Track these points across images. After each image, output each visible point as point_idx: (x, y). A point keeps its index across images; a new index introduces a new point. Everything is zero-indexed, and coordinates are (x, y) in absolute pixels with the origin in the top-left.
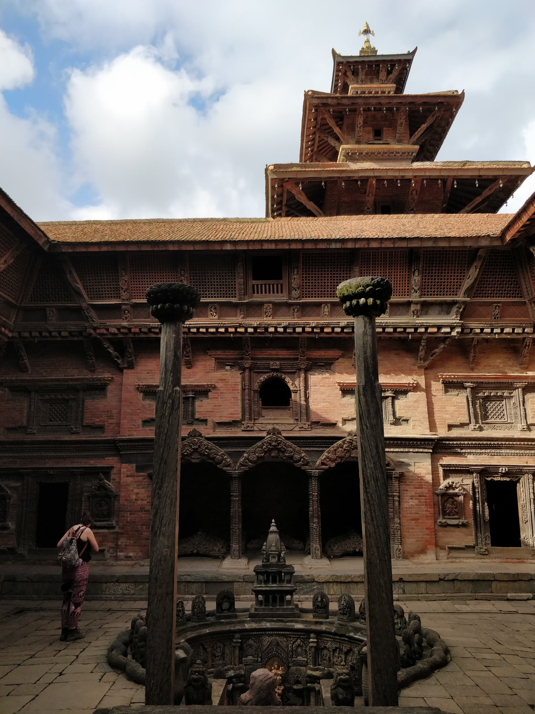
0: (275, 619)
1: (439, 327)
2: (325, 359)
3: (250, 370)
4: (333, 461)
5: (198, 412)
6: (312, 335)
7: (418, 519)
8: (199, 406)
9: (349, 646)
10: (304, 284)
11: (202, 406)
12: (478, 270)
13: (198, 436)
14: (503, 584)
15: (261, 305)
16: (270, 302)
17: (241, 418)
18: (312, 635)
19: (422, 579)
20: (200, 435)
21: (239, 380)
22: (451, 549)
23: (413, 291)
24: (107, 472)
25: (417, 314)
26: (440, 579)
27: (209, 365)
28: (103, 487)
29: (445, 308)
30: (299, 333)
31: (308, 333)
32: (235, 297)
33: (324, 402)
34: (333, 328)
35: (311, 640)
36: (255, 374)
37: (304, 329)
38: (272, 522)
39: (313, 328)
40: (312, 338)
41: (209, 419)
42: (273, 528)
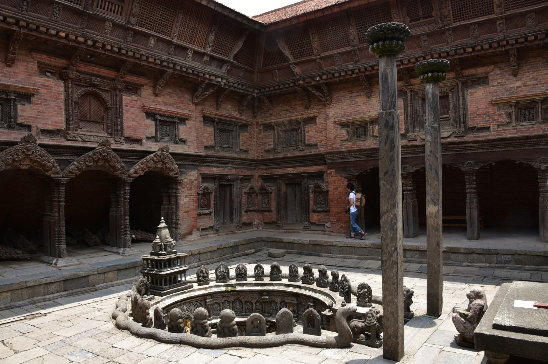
0: (179, 292)
1: (216, 77)
3: (72, 81)
5: (21, 116)
7: (188, 212)
8: (22, 110)
9: (237, 297)
10: (140, 14)
11: (25, 111)
13: (33, 142)
14: (244, 246)
15: (104, 20)
17: (65, 127)
18: (209, 297)
19: (210, 250)
21: (62, 89)
22: (203, 229)
23: (208, 46)
27: (31, 67)
32: (80, 5)
33: (133, 121)
35: (208, 300)
36: (74, 86)
37: (134, 53)
38: (161, 220)
39: (141, 55)
40: (136, 63)
41: (33, 125)
42: (163, 225)
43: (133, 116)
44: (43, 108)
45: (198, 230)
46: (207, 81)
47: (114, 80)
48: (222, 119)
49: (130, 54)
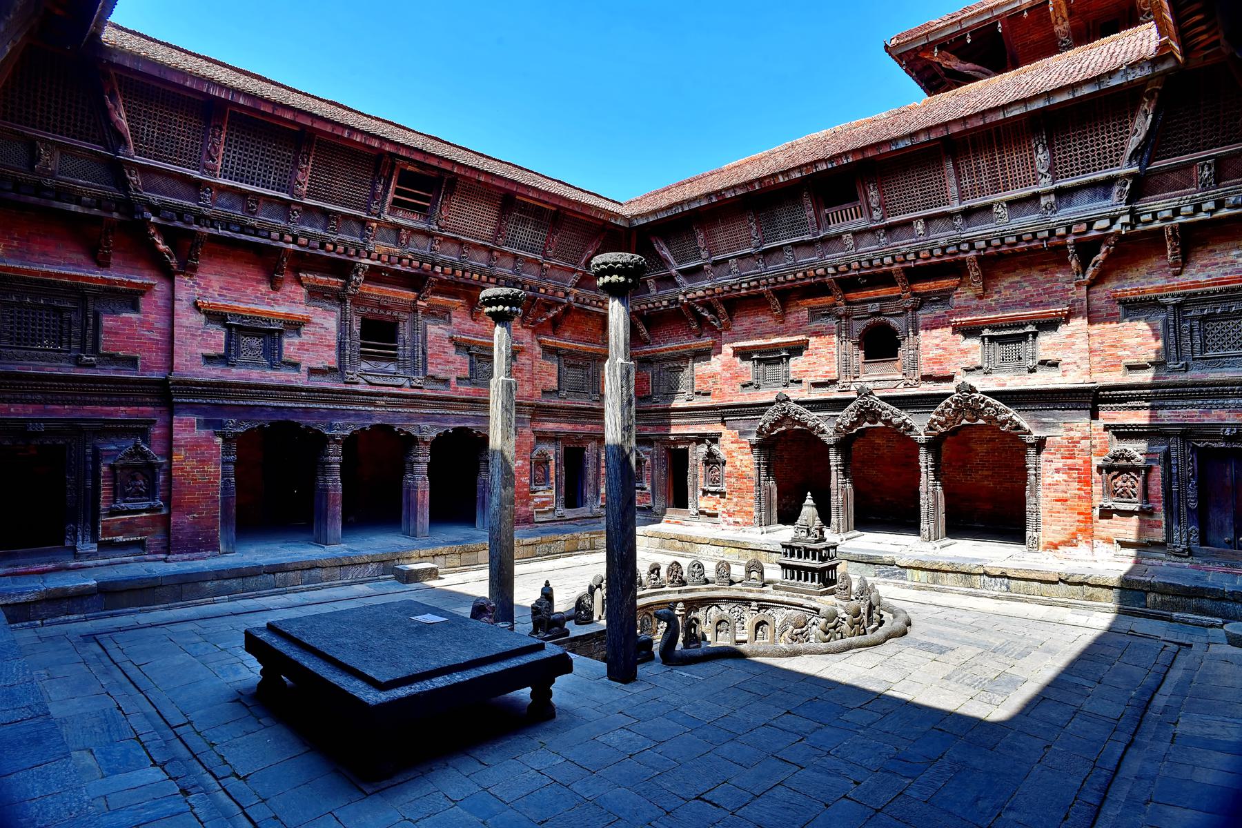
2: (939, 292)
3: (847, 317)
4: (942, 425)
6: (907, 265)
12: (1150, 116)
15: (838, 237)
16: (848, 232)
20: (788, 399)
24: (715, 438)
25: (1053, 208)
26: (1061, 580)
28: (710, 454)
29: (1100, 191)
30: (890, 265)
31: (901, 262)
34: (931, 251)
37: (893, 257)
39: (905, 255)
42: (809, 501)
43: (937, 341)
44: (813, 359)
45: (1109, 541)
46: (1070, 240)
47: (899, 297)
48: (1195, 294)
49: (888, 260)
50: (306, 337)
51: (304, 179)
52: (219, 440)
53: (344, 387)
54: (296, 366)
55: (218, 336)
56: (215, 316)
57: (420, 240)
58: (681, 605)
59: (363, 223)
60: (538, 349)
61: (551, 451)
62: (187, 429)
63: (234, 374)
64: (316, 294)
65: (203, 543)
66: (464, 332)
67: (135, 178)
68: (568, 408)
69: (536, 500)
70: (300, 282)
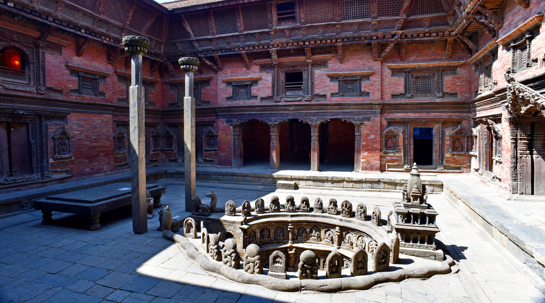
20: (512, 80)
50: (260, 85)
51: (240, 23)
52: (231, 127)
53: (274, 104)
54: (256, 97)
55: (230, 90)
56: (229, 83)
57: (297, 32)
58: (337, 228)
59: (268, 33)
60: (387, 72)
61: (399, 131)
62: (222, 123)
63: (236, 103)
64: (263, 67)
65: (227, 163)
66: (335, 70)
67: (196, 44)
68: (414, 104)
69: (388, 158)
70: (256, 64)
